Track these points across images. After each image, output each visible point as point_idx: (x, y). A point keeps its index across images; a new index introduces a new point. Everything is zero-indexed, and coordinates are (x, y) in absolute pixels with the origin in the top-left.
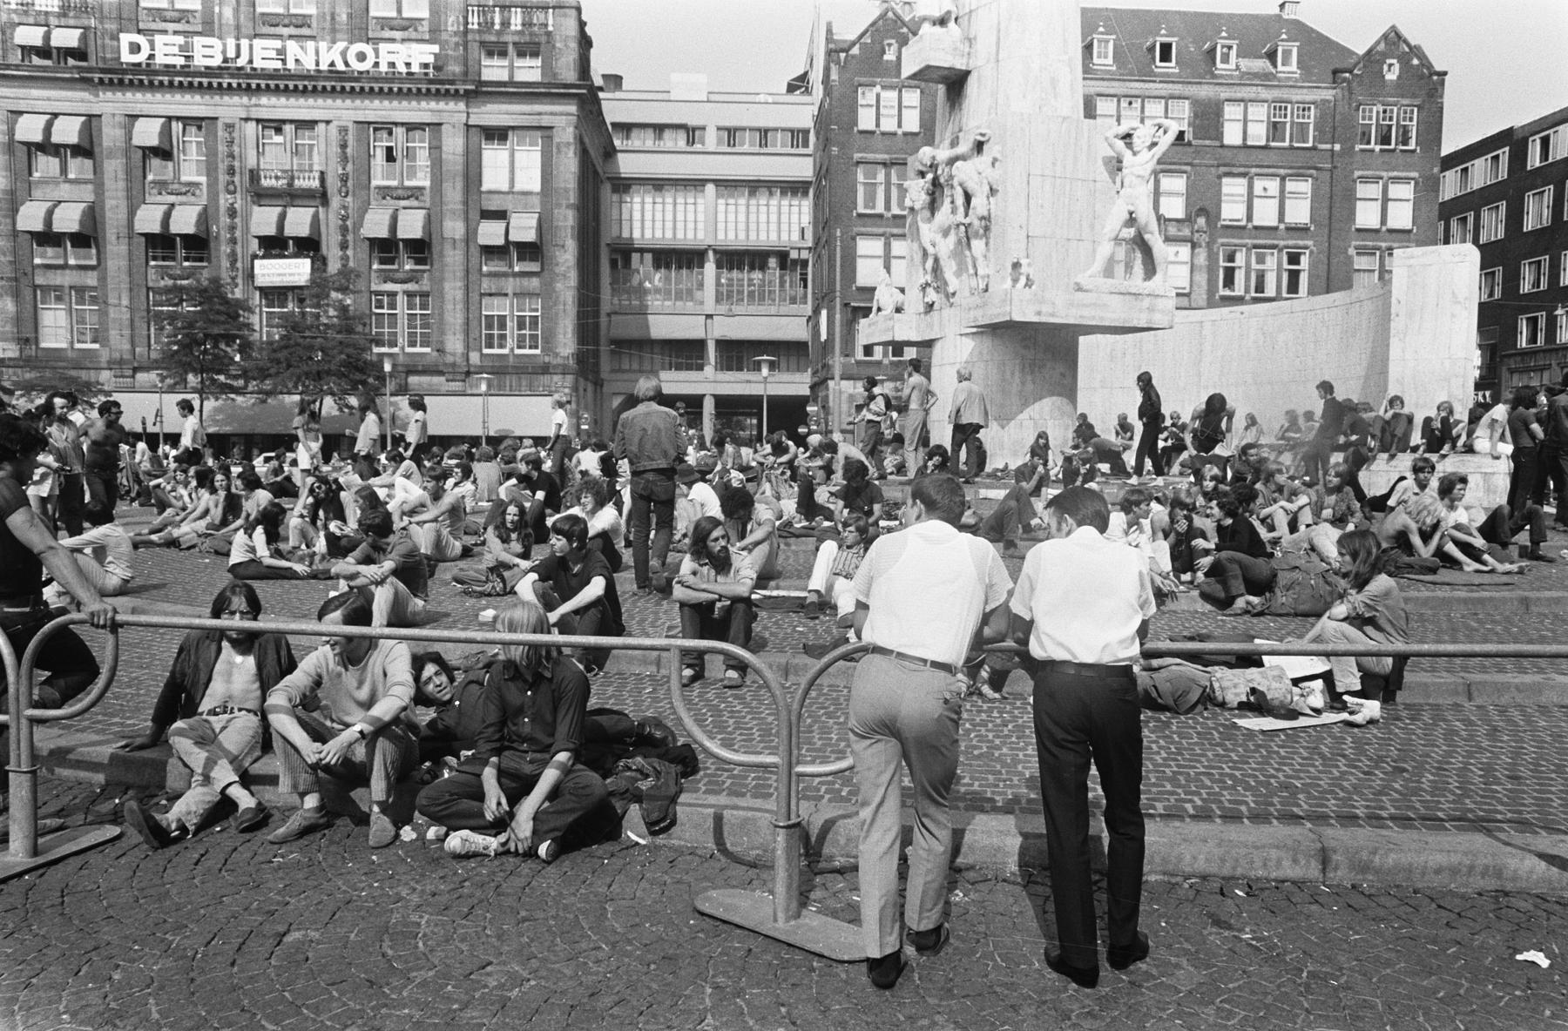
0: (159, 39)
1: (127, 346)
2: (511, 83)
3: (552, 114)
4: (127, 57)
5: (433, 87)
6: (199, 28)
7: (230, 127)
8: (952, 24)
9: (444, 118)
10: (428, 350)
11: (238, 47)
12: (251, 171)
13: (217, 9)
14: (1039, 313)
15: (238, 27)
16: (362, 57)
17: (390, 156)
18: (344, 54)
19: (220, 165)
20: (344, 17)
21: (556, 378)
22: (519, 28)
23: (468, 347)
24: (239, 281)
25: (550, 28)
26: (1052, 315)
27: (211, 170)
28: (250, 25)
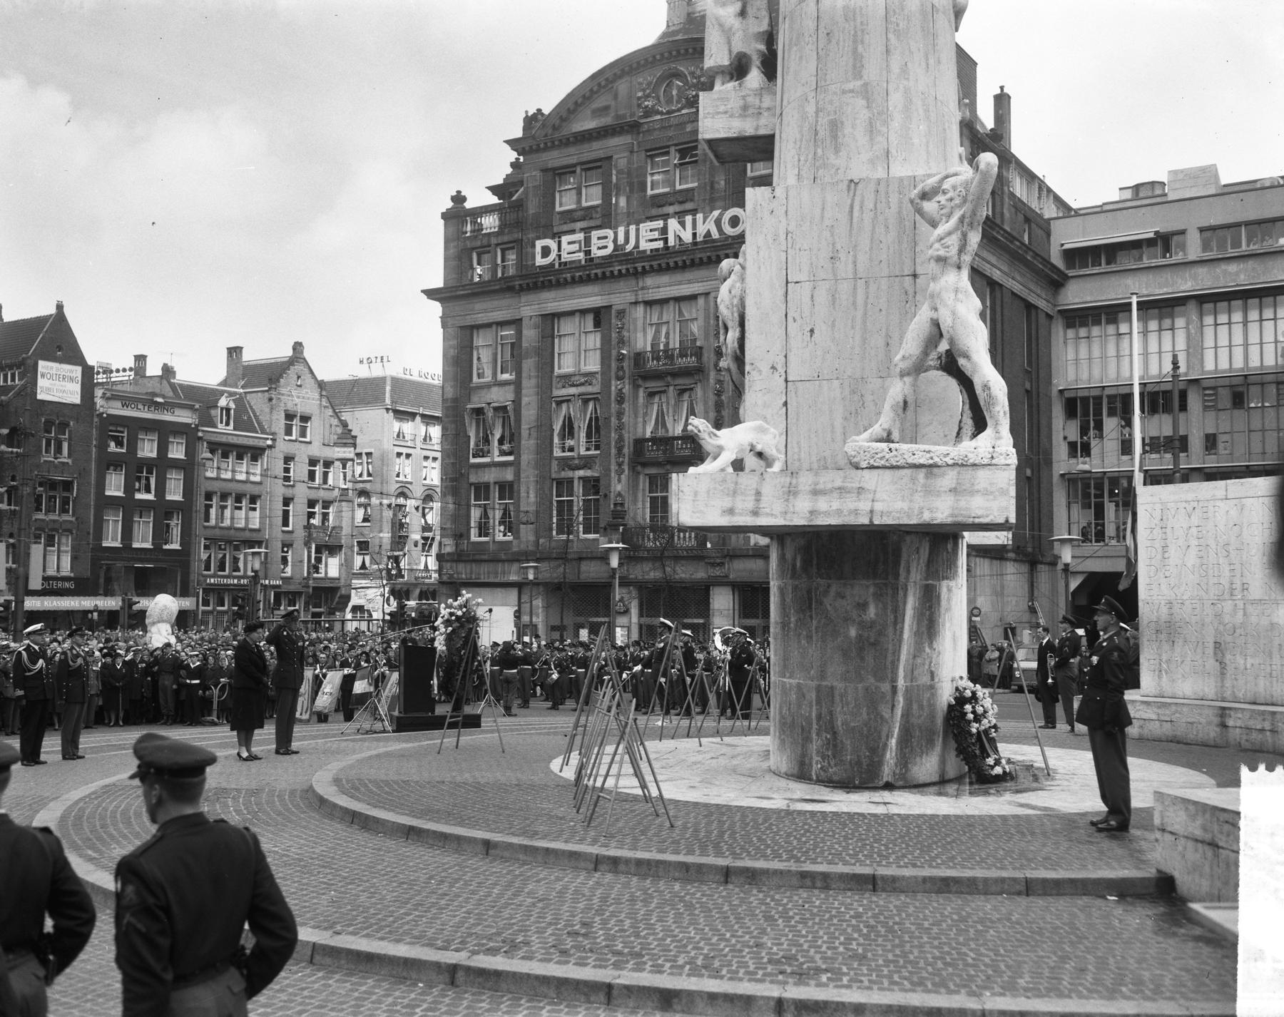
0: (565, 239)
1: (532, 538)
4: (540, 261)
6: (598, 222)
7: (621, 313)
8: (755, 77)
14: (731, 511)
18: (718, 223)
20: (723, 183)
24: (626, 467)
26: (755, 513)
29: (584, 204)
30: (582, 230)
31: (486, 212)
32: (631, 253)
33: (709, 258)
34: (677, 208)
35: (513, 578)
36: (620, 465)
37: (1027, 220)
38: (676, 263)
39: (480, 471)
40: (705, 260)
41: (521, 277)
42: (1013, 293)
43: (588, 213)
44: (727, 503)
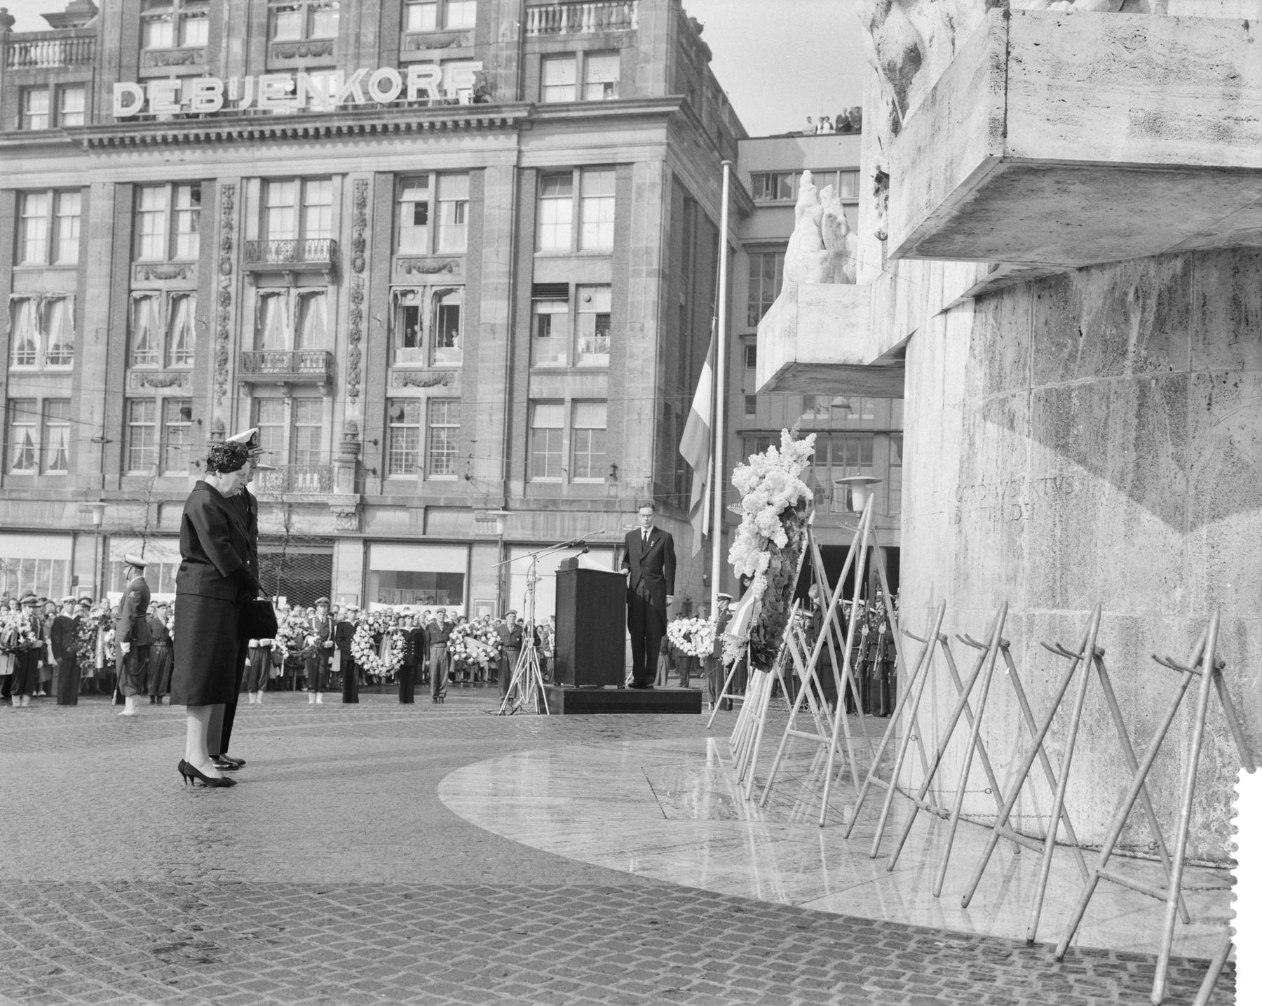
0: (153, 86)
1: (95, 473)
2: (581, 104)
3: (632, 145)
4: (119, 111)
5: (473, 118)
7: (229, 188)
9: (489, 160)
10: (454, 478)
11: (242, 86)
12: (251, 242)
13: (224, 44)
15: (247, 63)
16: (385, 85)
17: (420, 218)
18: (364, 84)
19: (216, 239)
21: (625, 517)
22: (592, 30)
23: (507, 476)
24: (228, 387)
25: (635, 26)
26: (1223, 133)
27: (205, 246)
28: (262, 58)
29: (185, 46)
30: (178, 77)
31: (44, 40)
32: (245, 112)
33: (350, 128)
34: (310, 61)
35: (66, 524)
36: (221, 384)
37: (720, 135)
38: (306, 130)
39: (23, 381)
40: (345, 130)
41: (92, 129)
42: (706, 216)
43: (189, 56)
44: (1145, 99)
